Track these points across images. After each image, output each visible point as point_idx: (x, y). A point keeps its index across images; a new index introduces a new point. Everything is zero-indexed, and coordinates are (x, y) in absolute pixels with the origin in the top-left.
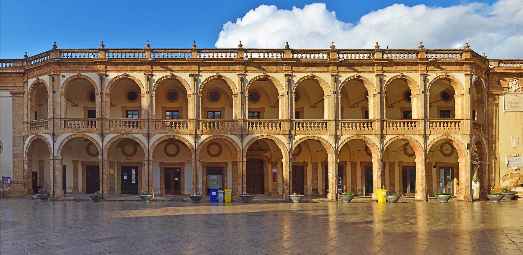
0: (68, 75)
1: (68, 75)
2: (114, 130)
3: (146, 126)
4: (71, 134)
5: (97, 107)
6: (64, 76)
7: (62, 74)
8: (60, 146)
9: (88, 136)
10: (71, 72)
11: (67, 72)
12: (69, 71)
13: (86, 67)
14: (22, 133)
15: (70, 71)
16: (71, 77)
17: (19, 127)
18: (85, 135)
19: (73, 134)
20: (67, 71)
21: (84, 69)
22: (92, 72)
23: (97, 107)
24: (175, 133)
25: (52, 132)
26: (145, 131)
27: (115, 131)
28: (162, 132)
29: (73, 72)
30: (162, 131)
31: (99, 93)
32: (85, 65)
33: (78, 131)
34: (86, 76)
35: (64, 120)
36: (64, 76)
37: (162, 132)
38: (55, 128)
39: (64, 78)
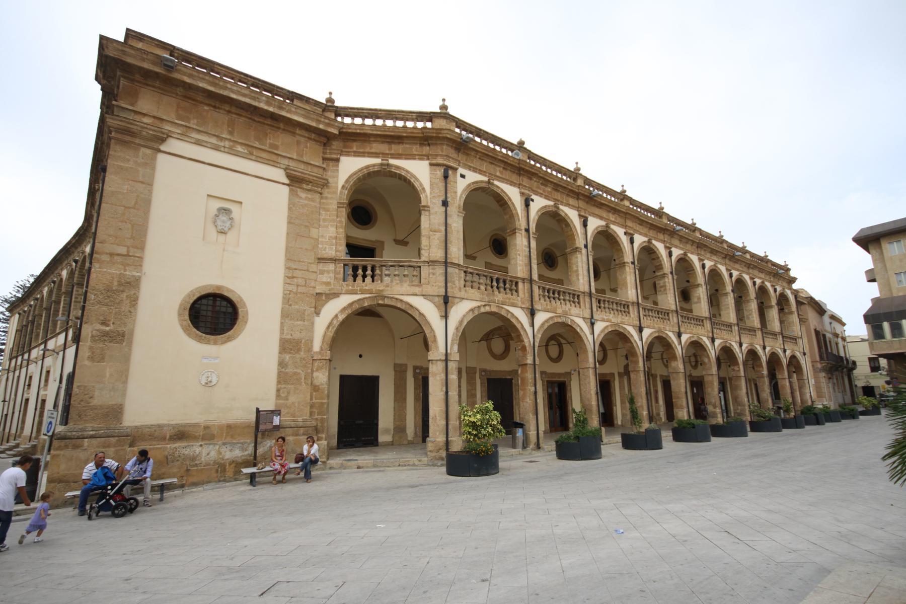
0: (473, 177)
1: (473, 177)
2: (547, 305)
3: (588, 305)
4: (479, 304)
5: (519, 255)
6: (463, 176)
7: (461, 171)
8: (457, 329)
9: (508, 311)
10: (476, 172)
11: (470, 170)
12: (474, 168)
13: (501, 172)
14: (313, 284)
15: (475, 170)
16: (477, 182)
17: (305, 268)
18: (503, 308)
19: (483, 303)
20: (471, 167)
21: (498, 174)
22: (511, 185)
23: (519, 255)
24: (619, 322)
25: (444, 294)
26: (587, 314)
27: (549, 307)
28: (606, 318)
29: (480, 173)
30: (606, 316)
31: (523, 228)
32: (500, 166)
33: (492, 298)
34: (502, 190)
35: (464, 269)
36: (463, 176)
37: (606, 318)
38: (449, 285)
39: (462, 179)
